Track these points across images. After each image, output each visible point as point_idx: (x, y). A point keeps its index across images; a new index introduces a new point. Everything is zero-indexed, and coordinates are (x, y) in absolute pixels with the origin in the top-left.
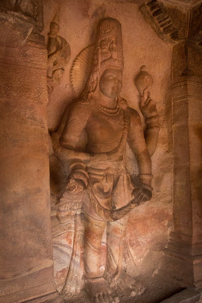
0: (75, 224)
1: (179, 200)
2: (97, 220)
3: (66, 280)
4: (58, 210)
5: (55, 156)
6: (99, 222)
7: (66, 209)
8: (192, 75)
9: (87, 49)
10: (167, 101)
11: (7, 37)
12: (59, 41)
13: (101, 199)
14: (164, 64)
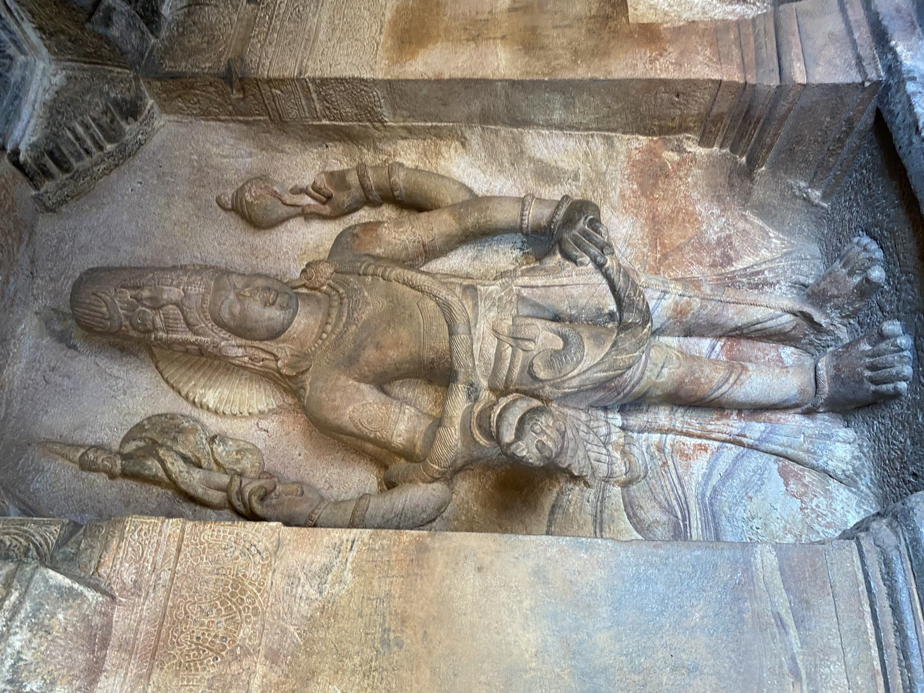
0: (651, 430)
1: (608, 117)
2: (643, 373)
3: (813, 468)
4: (608, 479)
5: (451, 478)
6: (650, 366)
7: (604, 458)
8: (243, 60)
9: (160, 365)
10: (320, 136)
11: (71, 649)
12: (131, 447)
13: (582, 359)
14: (212, 144)
